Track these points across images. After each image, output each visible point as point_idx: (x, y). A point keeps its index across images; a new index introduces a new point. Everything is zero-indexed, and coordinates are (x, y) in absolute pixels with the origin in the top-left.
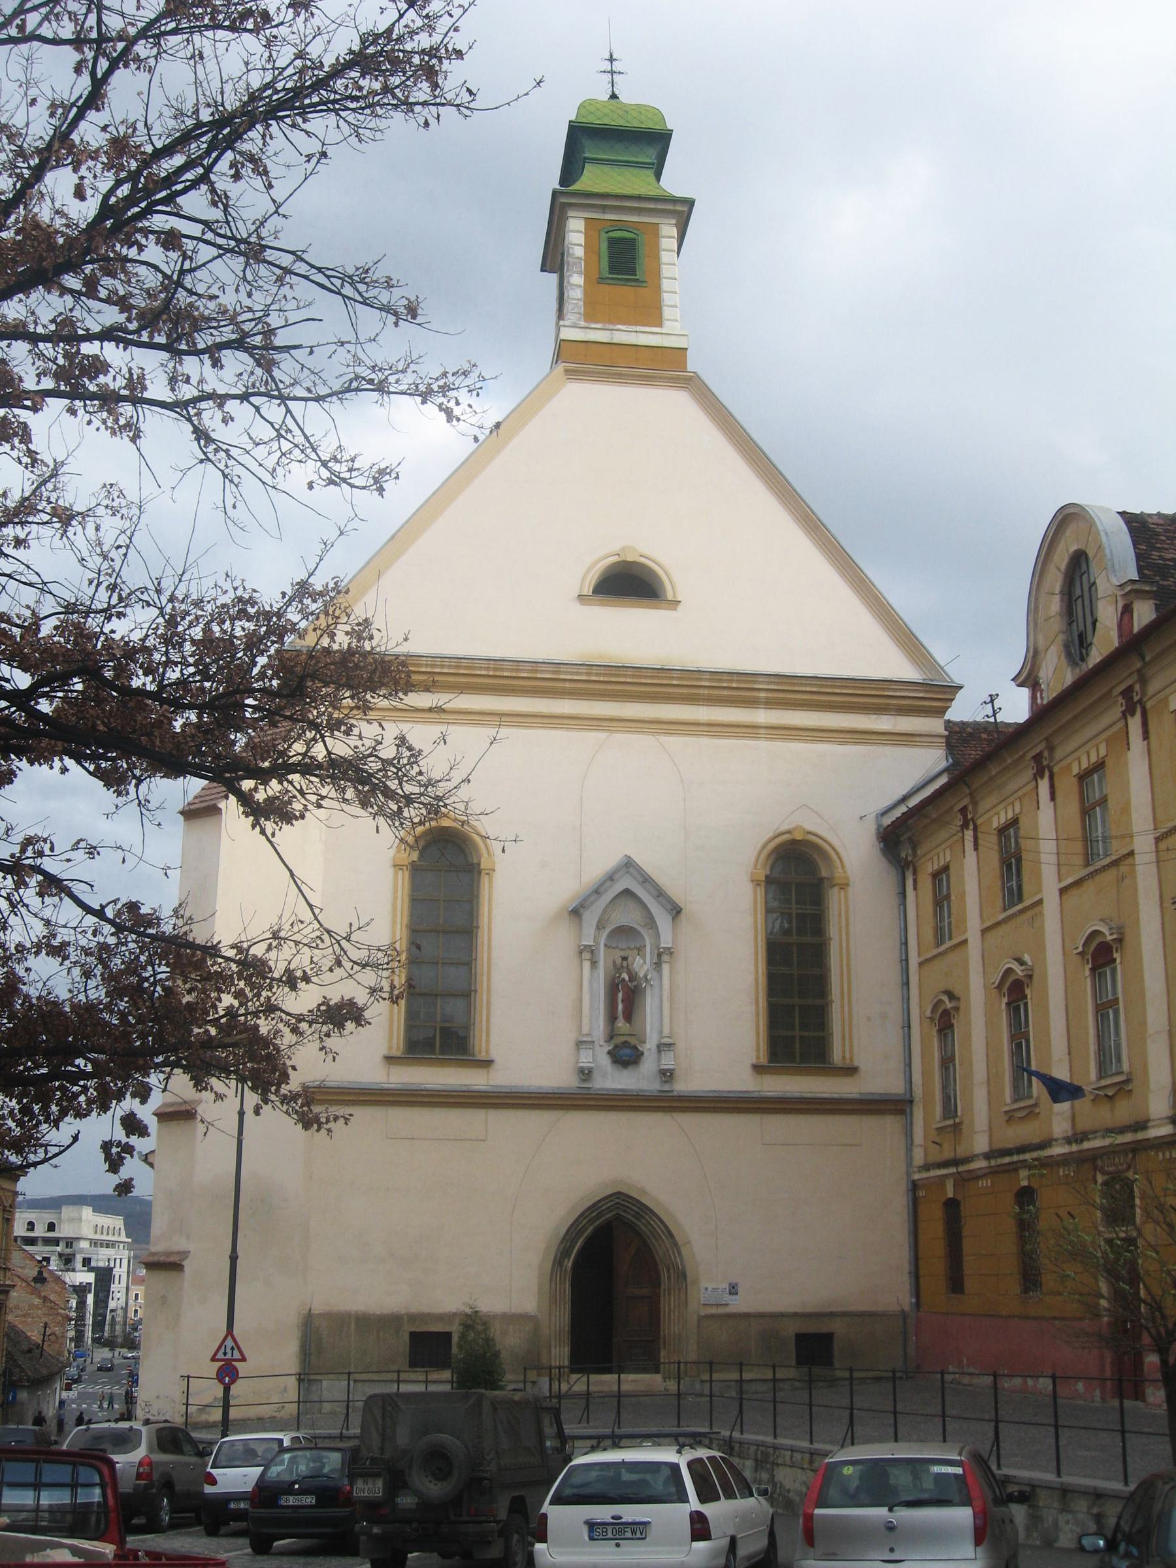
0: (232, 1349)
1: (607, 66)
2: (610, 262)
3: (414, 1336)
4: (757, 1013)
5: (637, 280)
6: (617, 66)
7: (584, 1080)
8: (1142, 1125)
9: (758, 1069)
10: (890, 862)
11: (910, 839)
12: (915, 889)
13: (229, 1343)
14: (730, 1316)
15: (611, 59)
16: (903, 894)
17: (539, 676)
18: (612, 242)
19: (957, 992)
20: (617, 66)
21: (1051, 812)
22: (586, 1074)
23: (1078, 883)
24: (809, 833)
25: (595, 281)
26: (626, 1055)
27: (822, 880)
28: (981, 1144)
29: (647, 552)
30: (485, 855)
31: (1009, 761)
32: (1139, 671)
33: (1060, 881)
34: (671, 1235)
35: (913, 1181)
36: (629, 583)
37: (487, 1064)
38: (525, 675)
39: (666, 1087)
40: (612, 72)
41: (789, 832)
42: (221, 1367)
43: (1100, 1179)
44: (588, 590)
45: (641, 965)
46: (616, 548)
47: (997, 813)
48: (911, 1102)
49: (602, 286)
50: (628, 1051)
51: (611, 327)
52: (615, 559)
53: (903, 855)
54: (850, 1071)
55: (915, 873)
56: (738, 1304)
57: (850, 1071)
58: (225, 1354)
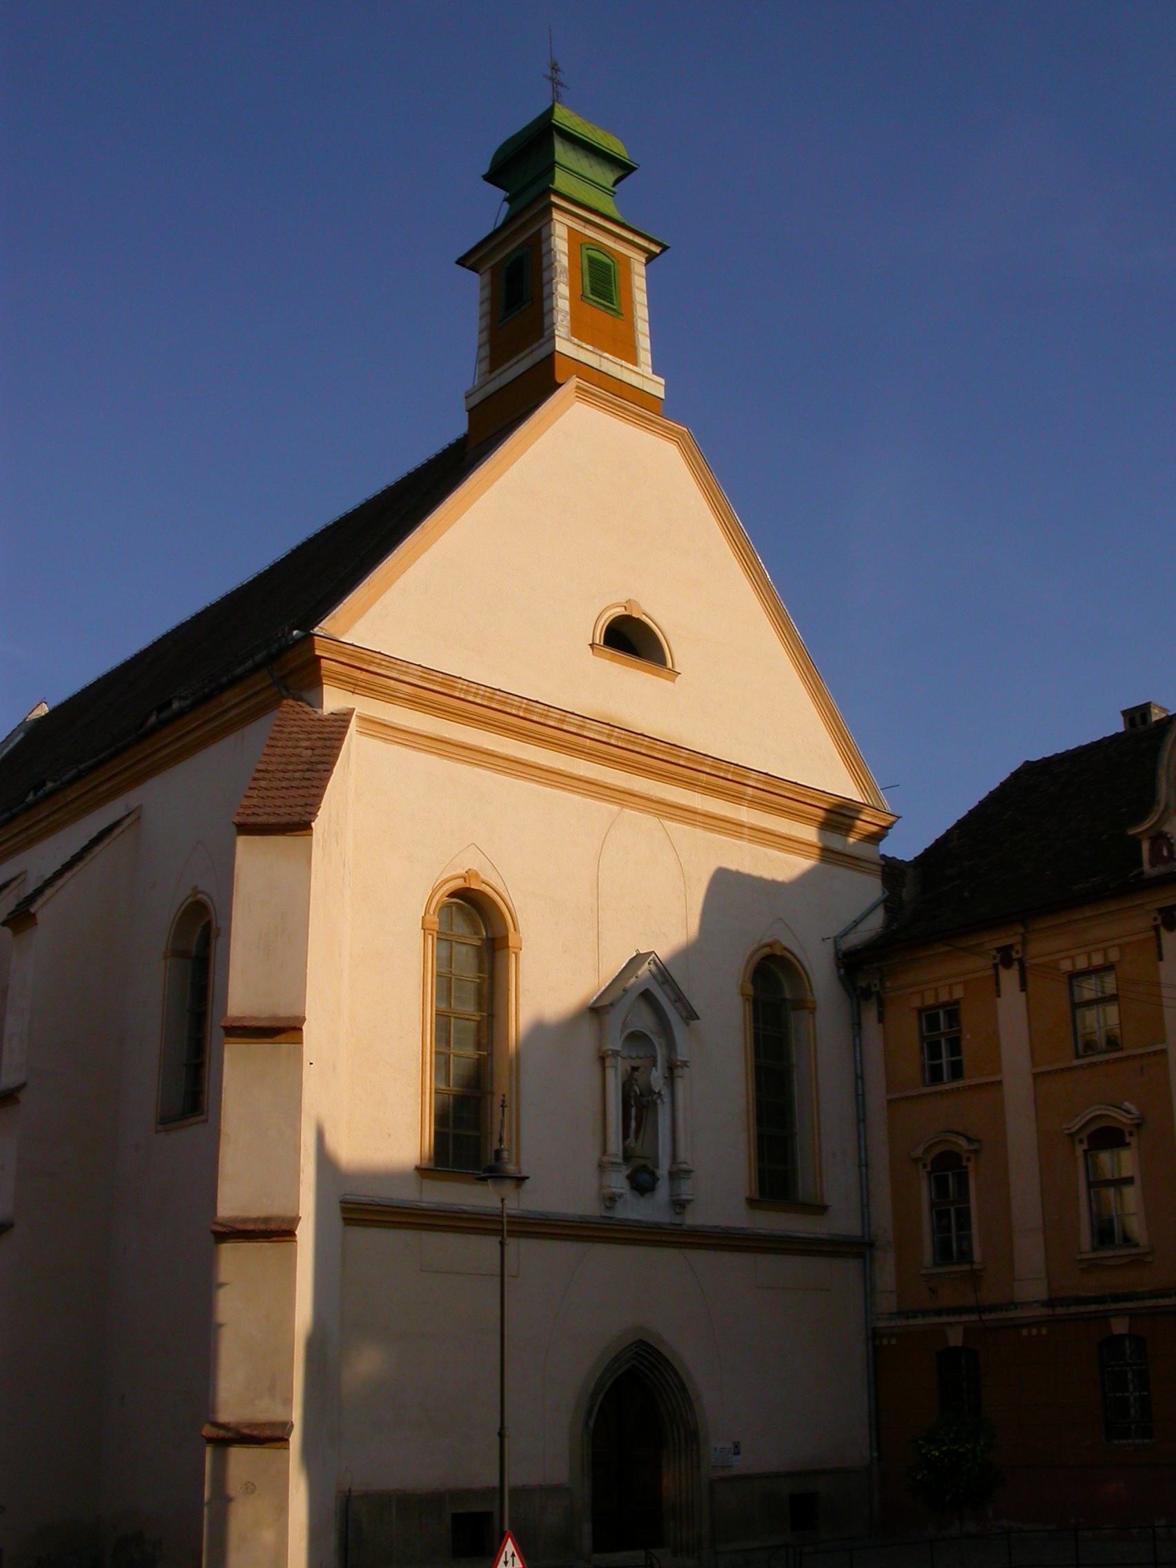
2: (591, 282)
3: (456, 1517)
5: (614, 310)
6: (561, 77)
7: (608, 1208)
9: (751, 1202)
10: (846, 990)
14: (738, 1478)
15: (555, 68)
16: (857, 1025)
17: (565, 727)
18: (592, 261)
22: (611, 1200)
24: (786, 949)
25: (577, 299)
26: (642, 1182)
27: (784, 1000)
29: (648, 611)
30: (512, 929)
34: (684, 1389)
35: (874, 1329)
38: (552, 724)
39: (678, 1220)
41: (770, 945)
44: (599, 639)
45: (657, 1077)
48: (871, 1245)
54: (820, 1209)
56: (741, 1465)
57: (820, 1209)
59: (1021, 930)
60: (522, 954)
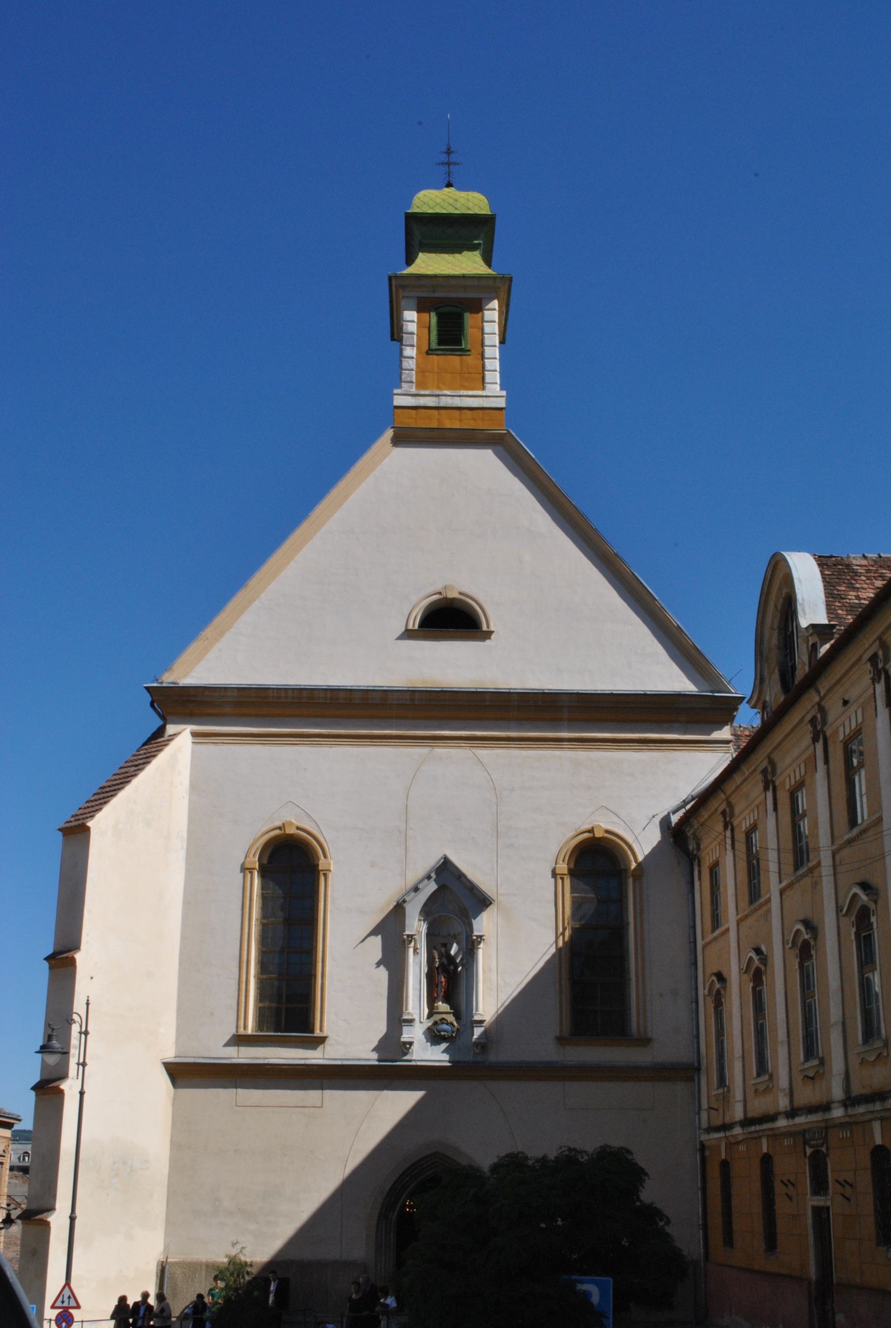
0: (69, 1297)
1: (444, 158)
4: (561, 992)
5: (462, 350)
6: (454, 158)
8: (826, 1107)
9: (561, 1040)
11: (694, 834)
12: (700, 879)
13: (67, 1292)
15: (449, 152)
19: (725, 975)
20: (454, 158)
21: (774, 821)
23: (790, 886)
24: (607, 831)
28: (738, 1114)
29: (465, 590)
31: (747, 774)
32: (819, 704)
33: (780, 882)
36: (450, 619)
37: (322, 1040)
39: (479, 1059)
40: (449, 164)
42: (59, 1314)
43: (809, 1151)
44: (414, 625)
46: (439, 587)
47: (745, 819)
48: (698, 1069)
49: (430, 356)
50: (445, 1027)
51: (438, 392)
52: (437, 597)
53: (691, 848)
54: (644, 1041)
55: (699, 866)
57: (644, 1041)
58: (63, 1302)
59: (723, 796)
60: (330, 875)
